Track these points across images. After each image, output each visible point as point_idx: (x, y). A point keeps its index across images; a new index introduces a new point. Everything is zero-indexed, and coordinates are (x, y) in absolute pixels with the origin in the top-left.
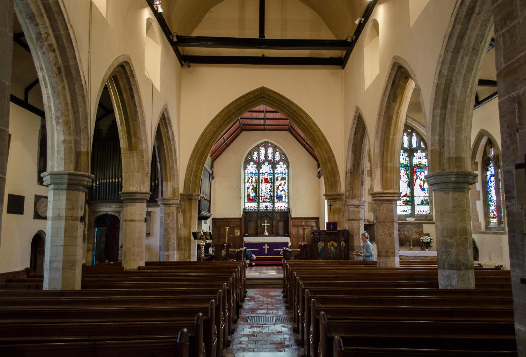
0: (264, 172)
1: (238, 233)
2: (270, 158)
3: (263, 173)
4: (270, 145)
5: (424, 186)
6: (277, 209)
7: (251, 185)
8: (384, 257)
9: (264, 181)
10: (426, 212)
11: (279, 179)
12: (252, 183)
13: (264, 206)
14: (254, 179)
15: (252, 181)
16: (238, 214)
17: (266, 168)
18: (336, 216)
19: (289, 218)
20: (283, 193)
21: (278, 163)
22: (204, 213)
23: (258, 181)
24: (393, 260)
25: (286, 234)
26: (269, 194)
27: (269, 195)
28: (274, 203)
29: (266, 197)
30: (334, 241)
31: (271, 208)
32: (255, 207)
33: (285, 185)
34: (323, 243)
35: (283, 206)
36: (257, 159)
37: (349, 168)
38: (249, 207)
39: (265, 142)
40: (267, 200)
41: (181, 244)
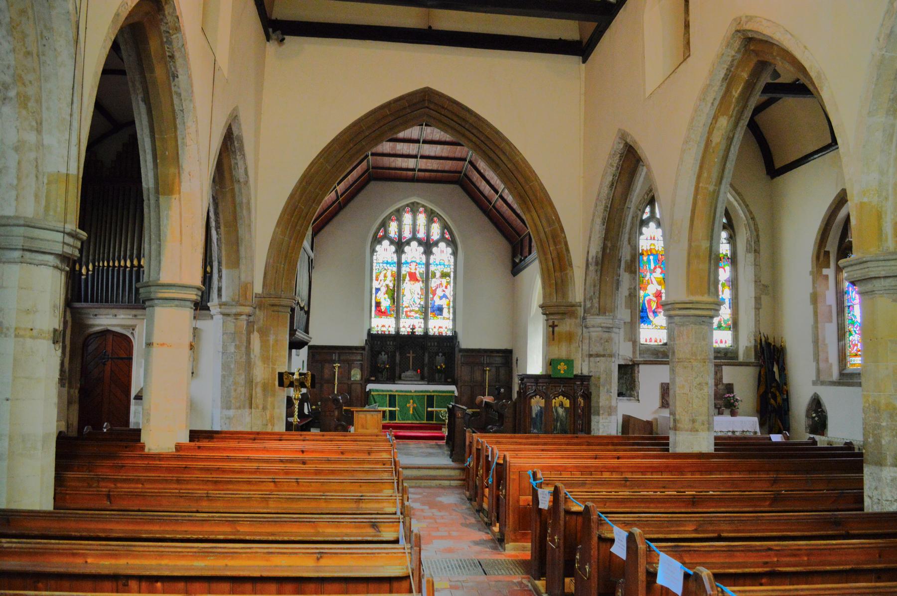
1: (356, 375)
2: (421, 235)
3: (408, 263)
4: (421, 209)
5: (723, 294)
6: (431, 333)
7: (384, 285)
8: (687, 431)
9: (408, 278)
10: (726, 342)
12: (385, 281)
13: (407, 326)
14: (389, 274)
15: (385, 276)
16: (359, 340)
17: (414, 252)
18: (564, 347)
19: (457, 349)
20: (444, 303)
21: (436, 244)
22: (300, 335)
23: (398, 278)
24: (704, 438)
25: (449, 380)
26: (418, 303)
27: (417, 305)
28: (426, 319)
30: (564, 396)
31: (420, 329)
32: (389, 327)
33: (448, 286)
34: (544, 400)
35: (444, 327)
36: (396, 236)
37: (594, 254)
38: (378, 326)
39: (413, 203)
40: (412, 314)
41: (256, 394)
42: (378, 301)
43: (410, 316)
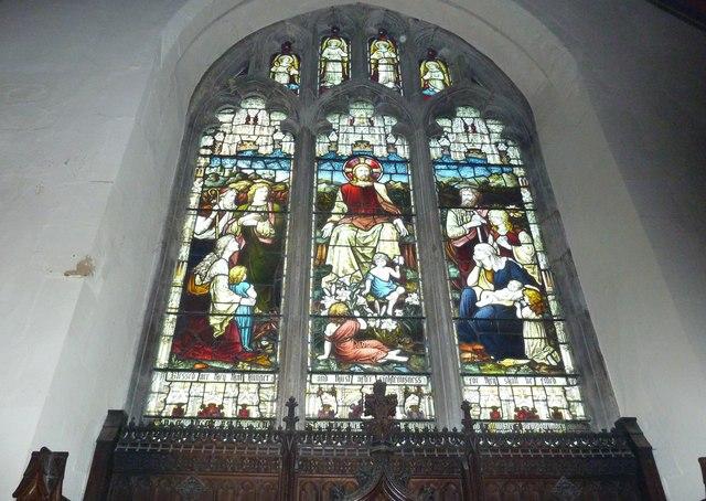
0: (344, 151)
3: (339, 159)
7: (235, 227)
9: (340, 206)
11: (468, 196)
12: (238, 214)
14: (260, 195)
15: (243, 200)
26: (393, 299)
29: (363, 325)
33: (523, 236)
40: (369, 349)
42: (200, 291)
43: (357, 360)
